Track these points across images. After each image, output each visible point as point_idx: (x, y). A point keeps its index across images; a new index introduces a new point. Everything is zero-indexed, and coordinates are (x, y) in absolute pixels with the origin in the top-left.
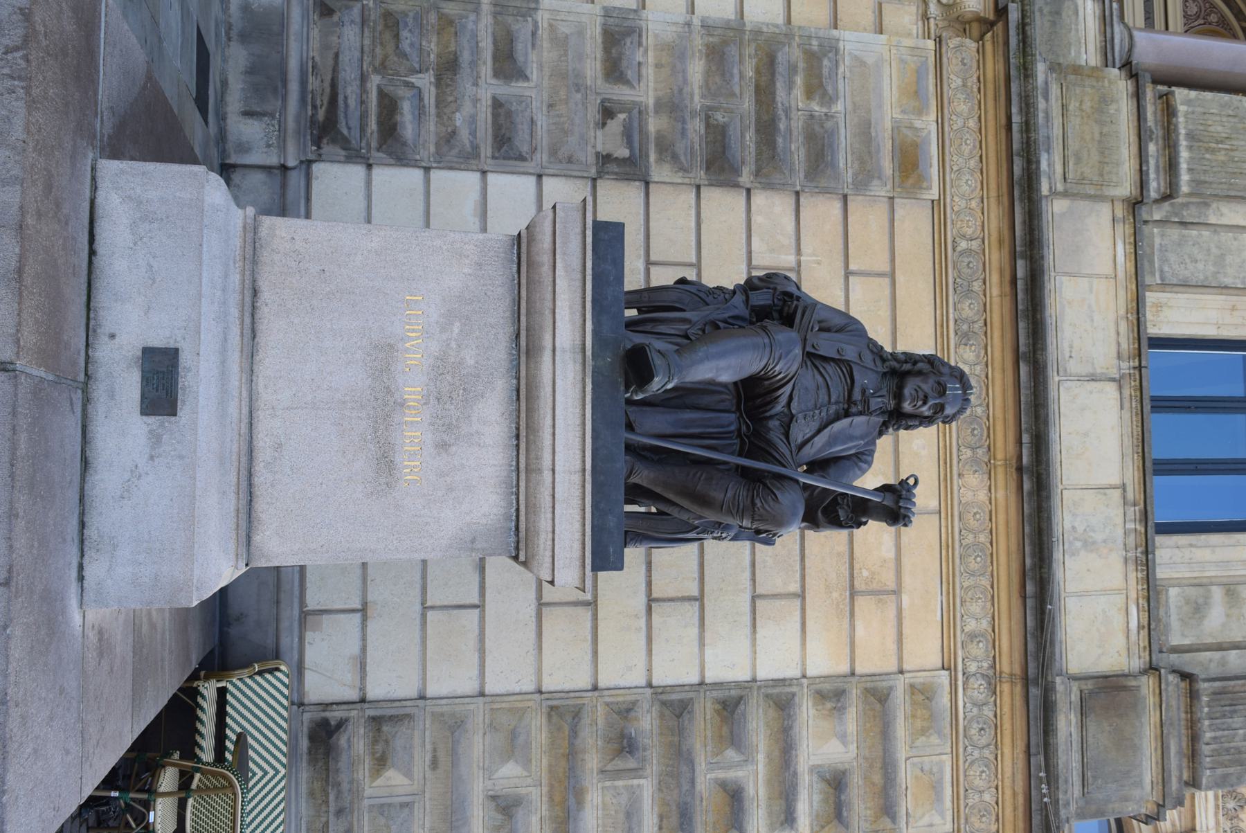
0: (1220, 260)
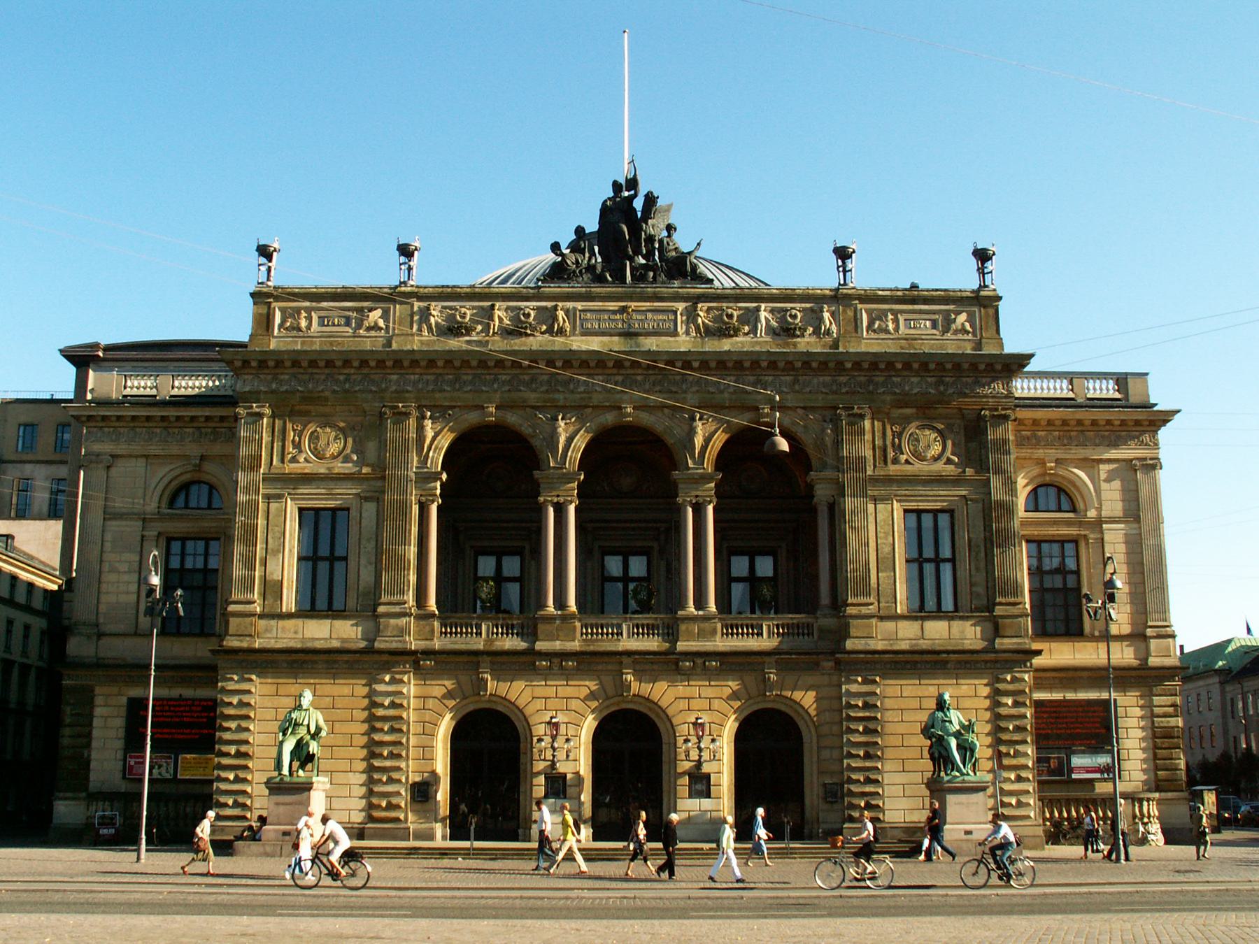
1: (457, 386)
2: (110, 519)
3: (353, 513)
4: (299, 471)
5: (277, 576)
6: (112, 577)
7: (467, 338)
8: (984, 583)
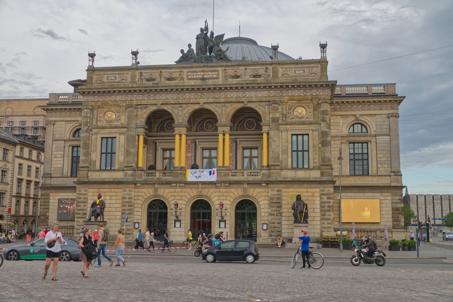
0: (285, 159)
1: (149, 98)
2: (55, 141)
3: (117, 139)
4: (101, 126)
5: (94, 159)
6: (56, 159)
7: (152, 82)
8: (318, 158)
